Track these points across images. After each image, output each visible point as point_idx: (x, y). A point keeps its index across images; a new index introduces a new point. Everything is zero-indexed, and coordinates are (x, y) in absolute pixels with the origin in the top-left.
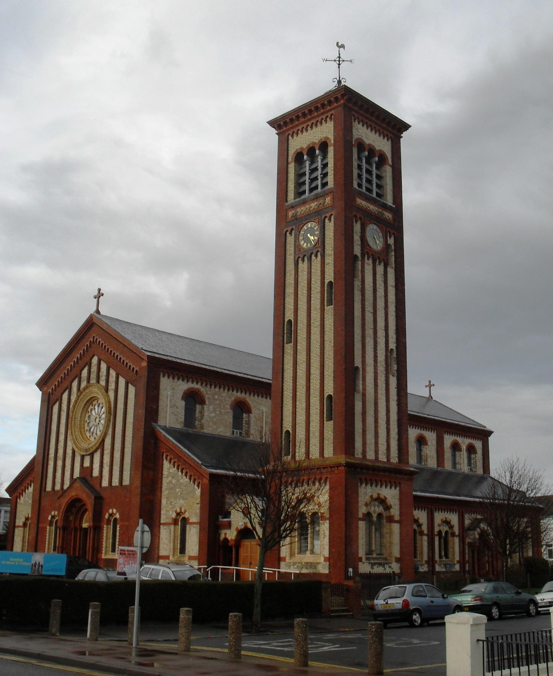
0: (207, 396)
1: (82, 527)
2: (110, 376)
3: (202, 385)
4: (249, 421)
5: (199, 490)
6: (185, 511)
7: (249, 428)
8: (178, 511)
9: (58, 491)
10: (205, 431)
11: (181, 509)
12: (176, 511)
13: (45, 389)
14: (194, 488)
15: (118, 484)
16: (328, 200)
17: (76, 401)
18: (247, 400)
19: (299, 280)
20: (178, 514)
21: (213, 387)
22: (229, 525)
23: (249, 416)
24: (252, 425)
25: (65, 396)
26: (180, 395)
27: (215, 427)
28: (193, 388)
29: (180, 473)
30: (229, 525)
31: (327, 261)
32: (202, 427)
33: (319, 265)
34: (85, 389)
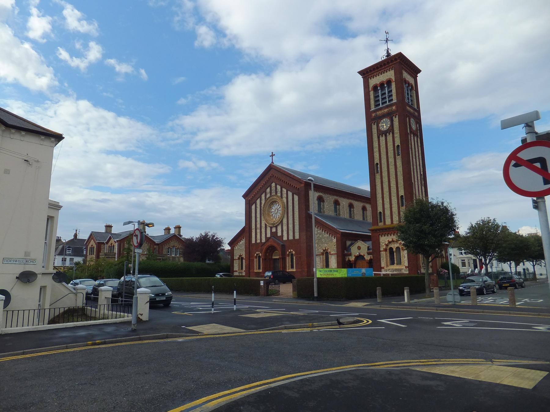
0: (325, 198)
1: (272, 258)
2: (283, 191)
3: (323, 193)
4: (340, 209)
5: (335, 239)
6: (328, 249)
7: (340, 212)
8: (324, 249)
9: (259, 243)
10: (326, 214)
11: (325, 248)
12: (323, 249)
13: (247, 198)
14: (332, 239)
15: (292, 239)
16: (394, 108)
17: (265, 203)
18: (339, 199)
19: (381, 145)
20: (324, 250)
21: (327, 194)
22: (350, 255)
23: (339, 207)
24: (341, 210)
25: (258, 201)
26: (316, 198)
27: (328, 212)
28: (320, 195)
29: (324, 232)
30: (350, 255)
31: (395, 136)
32: (324, 212)
33: (391, 138)
34: (269, 197)
